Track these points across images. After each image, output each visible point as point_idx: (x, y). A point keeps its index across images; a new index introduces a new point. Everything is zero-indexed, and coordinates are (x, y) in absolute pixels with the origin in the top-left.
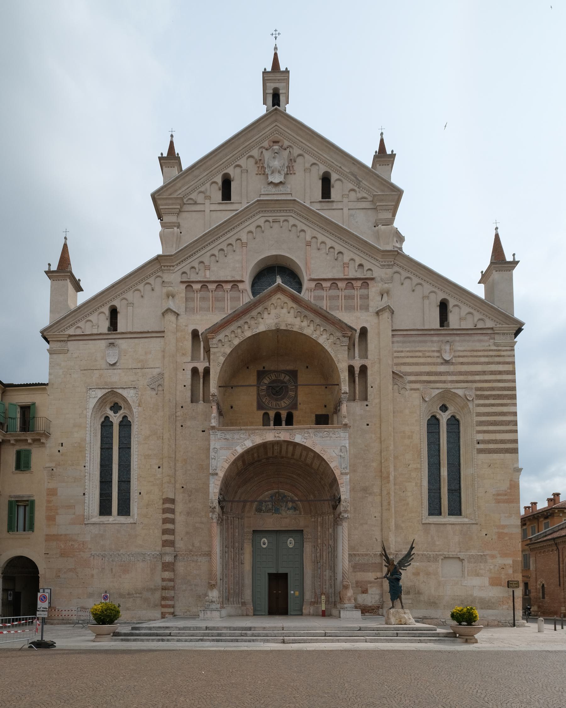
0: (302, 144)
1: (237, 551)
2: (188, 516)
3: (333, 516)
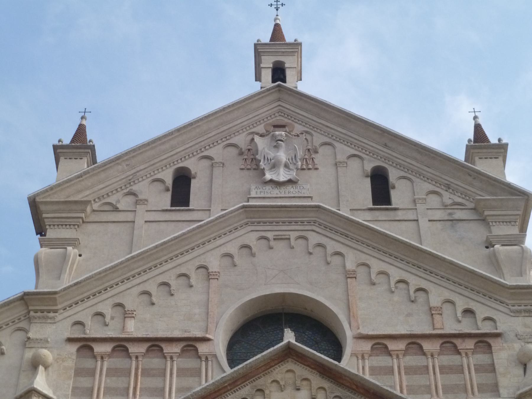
0: (329, 130)
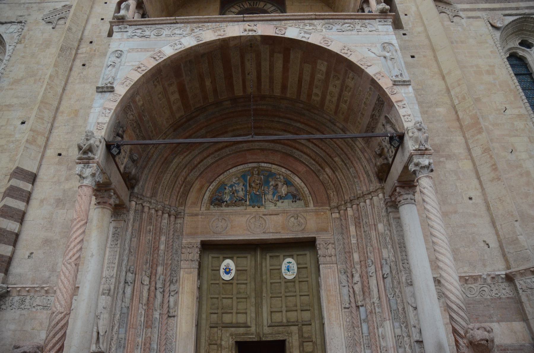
1: (159, 285)
2: (57, 206)
3: (381, 195)
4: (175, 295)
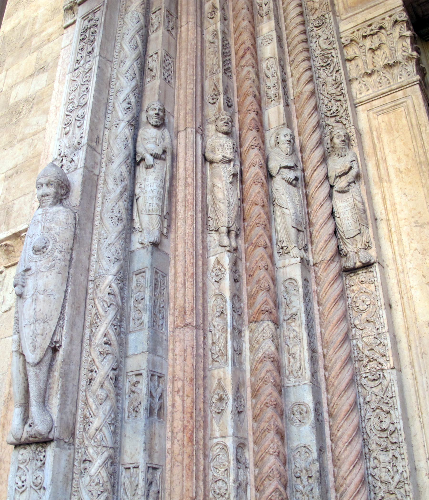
4: (354, 188)
